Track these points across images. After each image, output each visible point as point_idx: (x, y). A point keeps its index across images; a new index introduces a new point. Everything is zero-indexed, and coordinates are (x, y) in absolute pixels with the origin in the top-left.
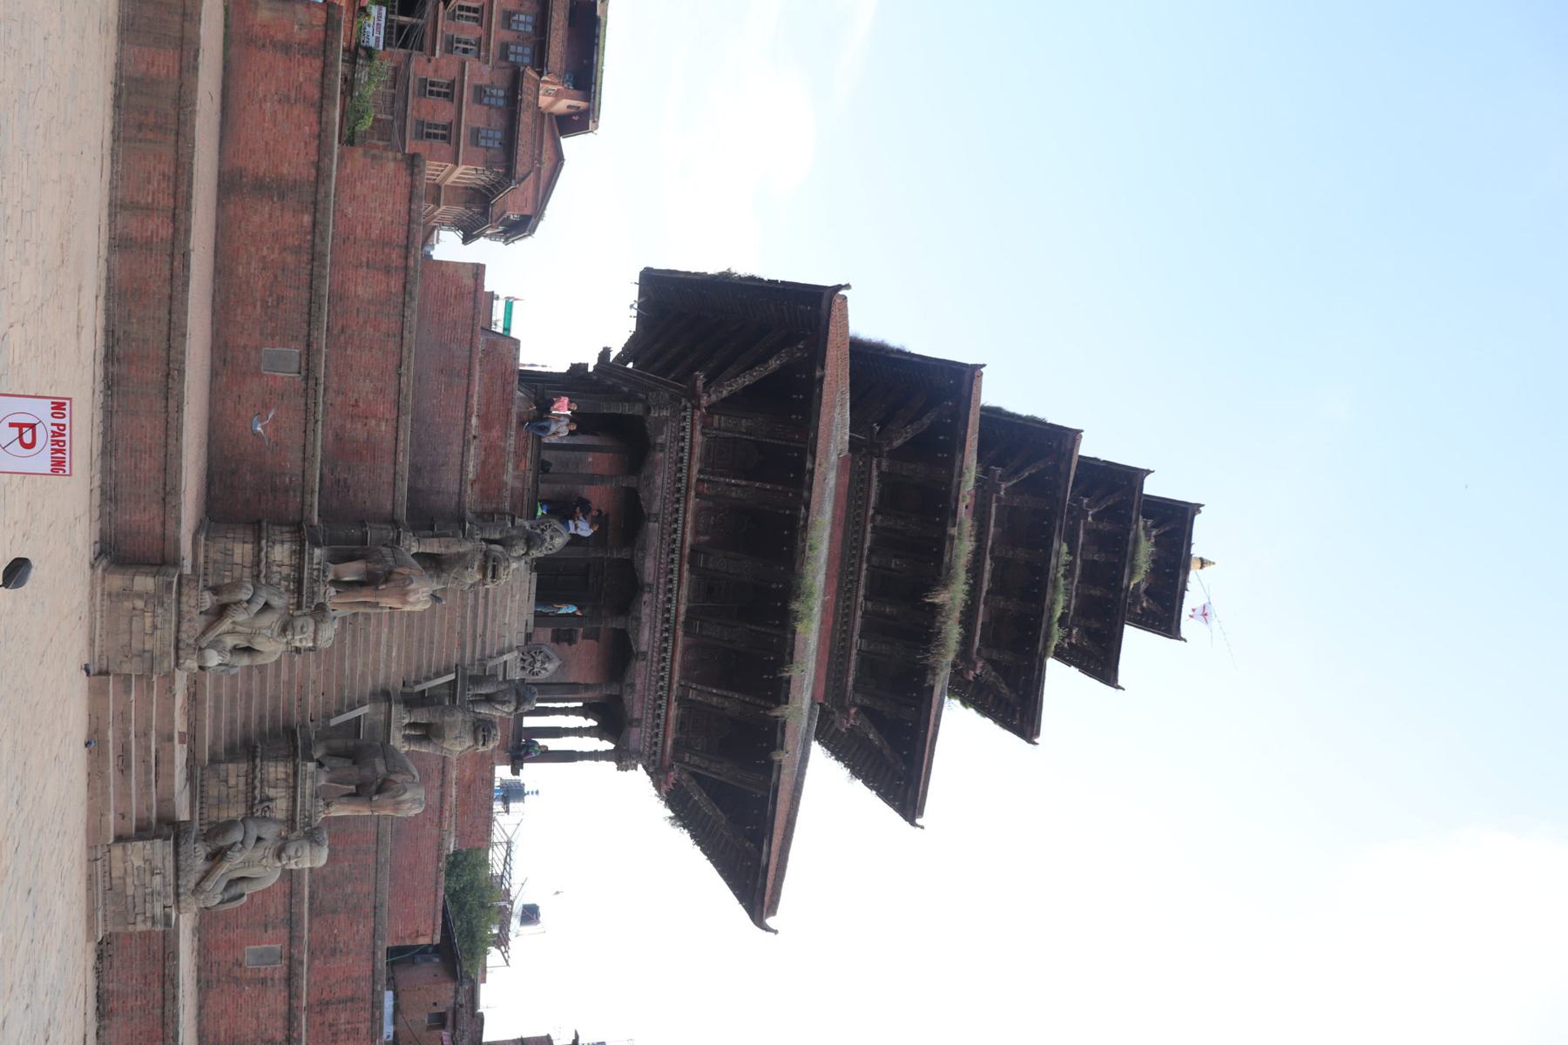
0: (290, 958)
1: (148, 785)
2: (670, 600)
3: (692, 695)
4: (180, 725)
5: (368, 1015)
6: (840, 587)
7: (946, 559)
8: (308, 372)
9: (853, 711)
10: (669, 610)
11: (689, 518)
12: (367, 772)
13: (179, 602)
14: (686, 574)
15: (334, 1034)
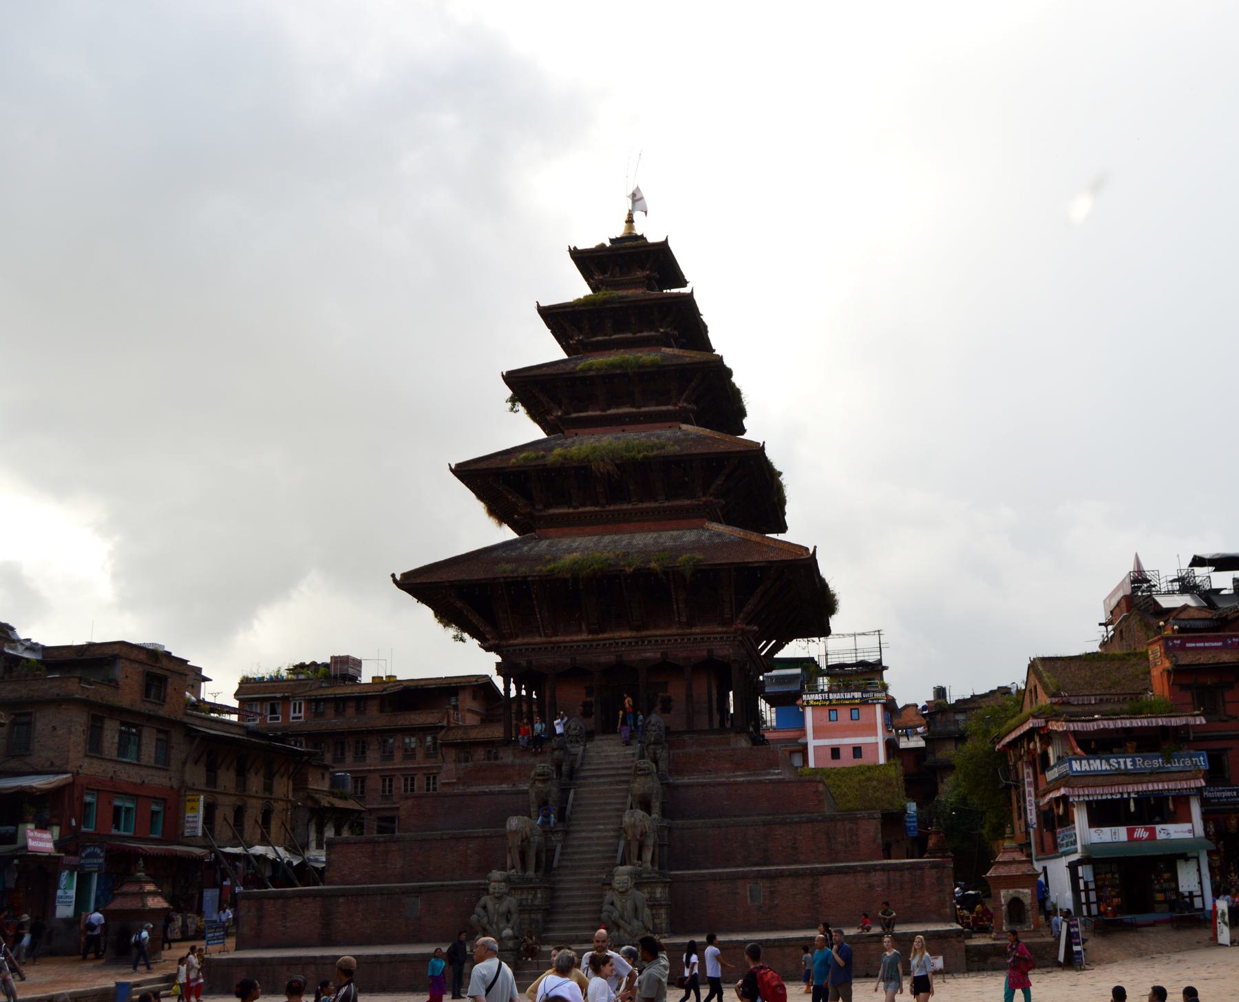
3: (684, 619)
11: (568, 639)
14: (606, 635)
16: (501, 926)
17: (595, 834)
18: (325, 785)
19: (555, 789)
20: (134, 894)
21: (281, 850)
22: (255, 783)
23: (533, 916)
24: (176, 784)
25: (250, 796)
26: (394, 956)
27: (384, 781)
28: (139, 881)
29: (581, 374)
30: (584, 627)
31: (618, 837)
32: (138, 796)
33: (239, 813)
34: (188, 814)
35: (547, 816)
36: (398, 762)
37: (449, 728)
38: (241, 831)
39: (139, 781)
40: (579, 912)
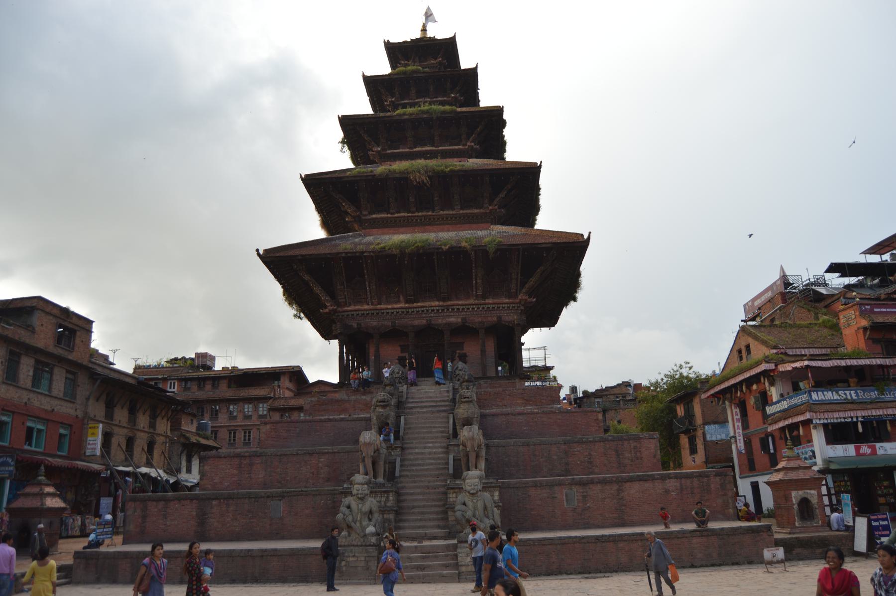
0: (571, 484)
1: (436, 557)
2: (433, 310)
3: (480, 293)
4: (415, 544)
5: (626, 443)
6: (429, 225)
7: (398, 176)
8: (281, 496)
9: (490, 208)
10: (438, 310)
11: (390, 307)
12: (462, 454)
13: (344, 546)
14: (419, 304)
15: (637, 459)
16: (365, 523)
17: (427, 450)
18: (193, 428)
19: (393, 414)
20: (35, 495)
21: (161, 472)
22: (143, 421)
23: (386, 516)
24: (80, 414)
25: (138, 430)
26: (266, 550)
27: (230, 433)
28: (40, 484)
29: (398, 118)
30: (401, 298)
31: (447, 453)
32: (48, 420)
33: (130, 442)
34: (90, 438)
35: (387, 435)
36: (240, 421)
37: (275, 399)
38: (131, 456)
39: (49, 409)
40: (423, 513)
